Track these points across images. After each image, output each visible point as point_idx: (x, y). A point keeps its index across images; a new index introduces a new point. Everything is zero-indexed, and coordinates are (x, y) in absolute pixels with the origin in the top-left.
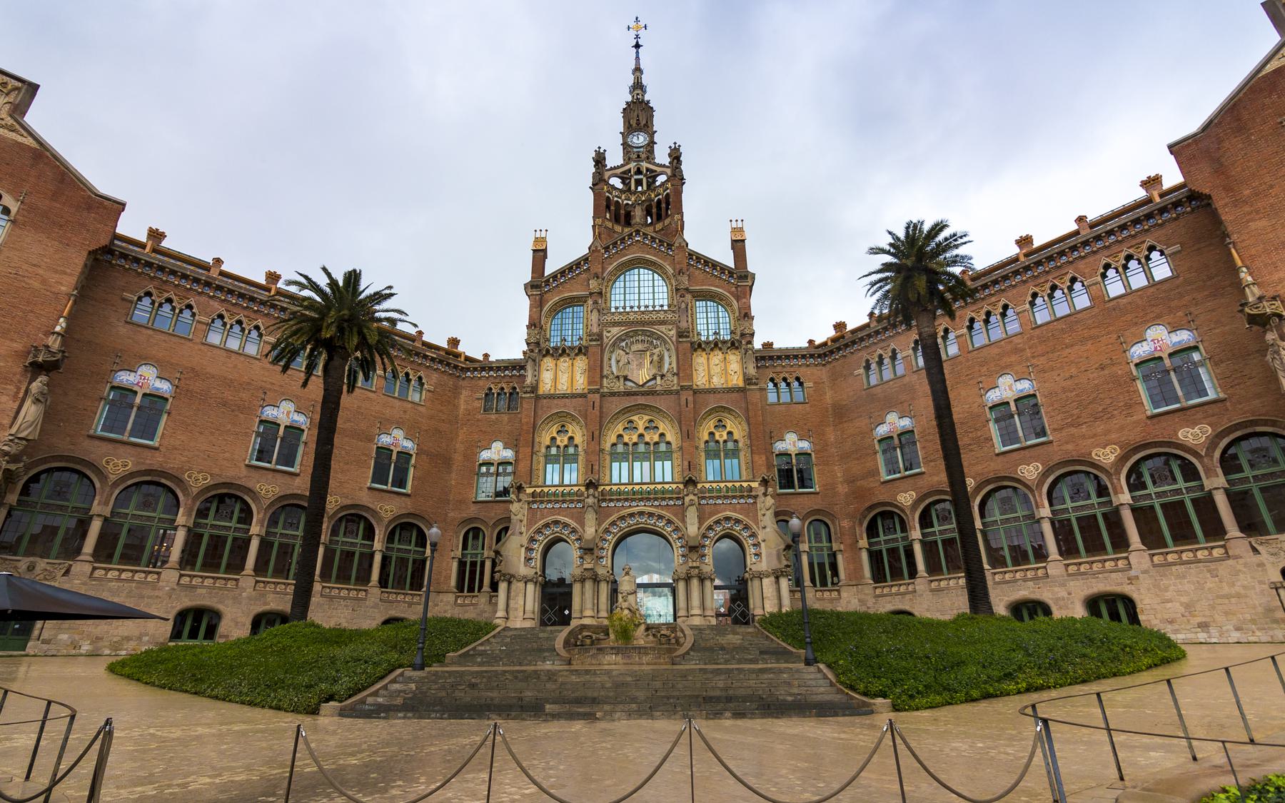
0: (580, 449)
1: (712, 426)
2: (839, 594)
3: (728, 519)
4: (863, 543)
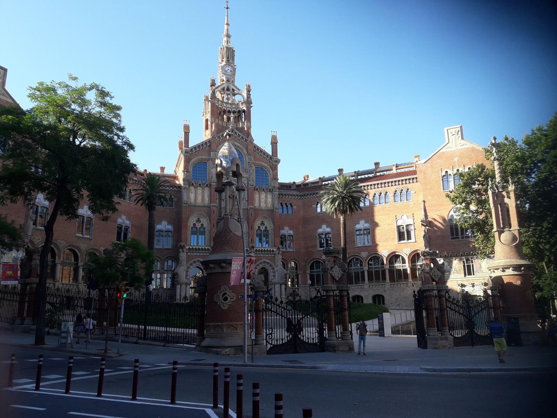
0: (206, 230)
1: (259, 224)
2: (298, 290)
3: (265, 262)
4: (308, 271)
